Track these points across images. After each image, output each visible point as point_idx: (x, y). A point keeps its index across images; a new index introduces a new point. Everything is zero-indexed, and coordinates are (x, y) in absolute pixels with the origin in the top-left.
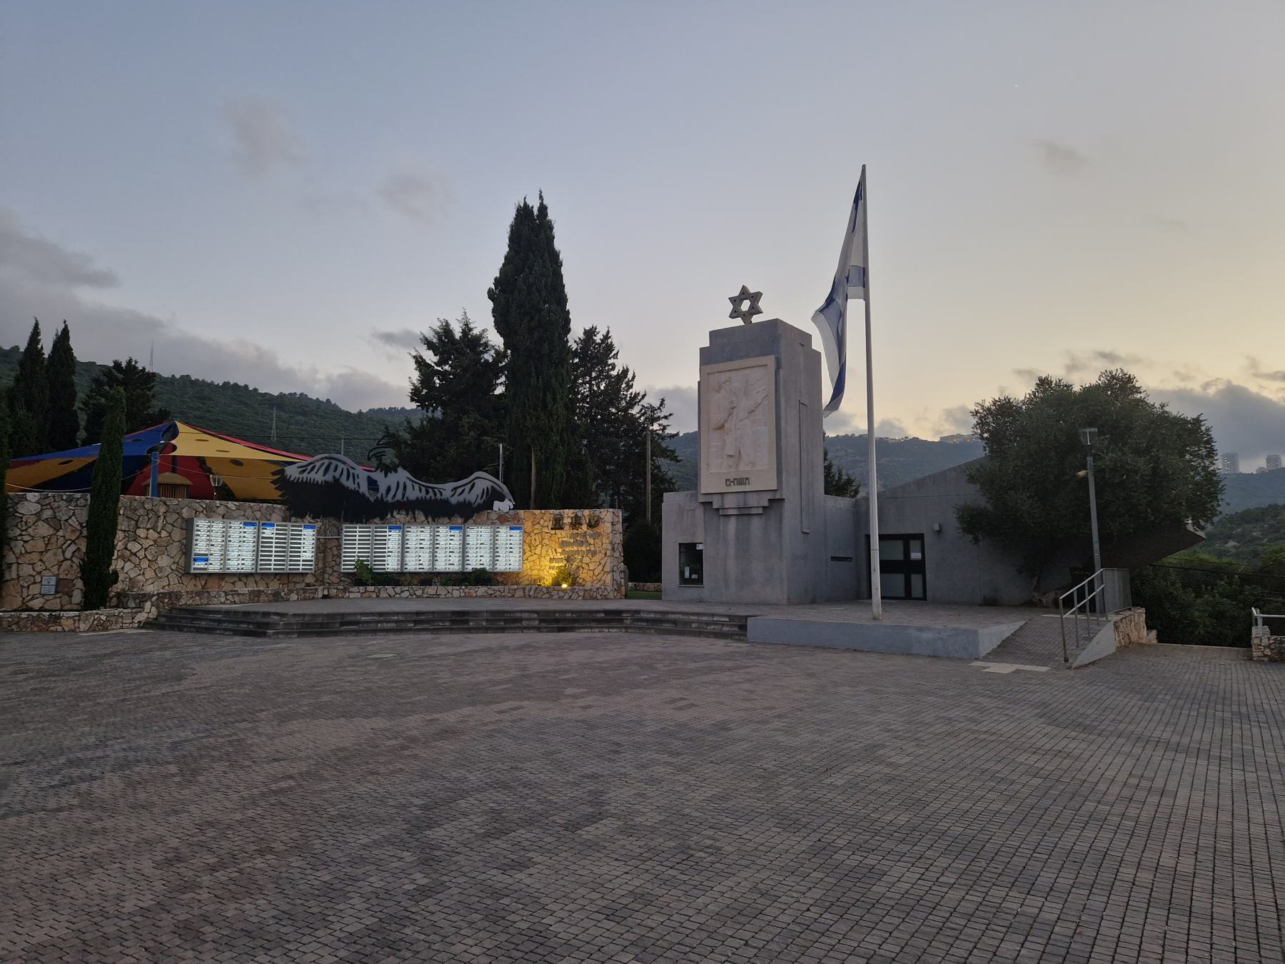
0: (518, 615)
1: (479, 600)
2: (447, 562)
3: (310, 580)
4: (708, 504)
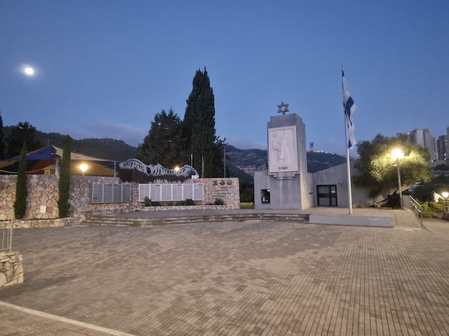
0: (224, 216)
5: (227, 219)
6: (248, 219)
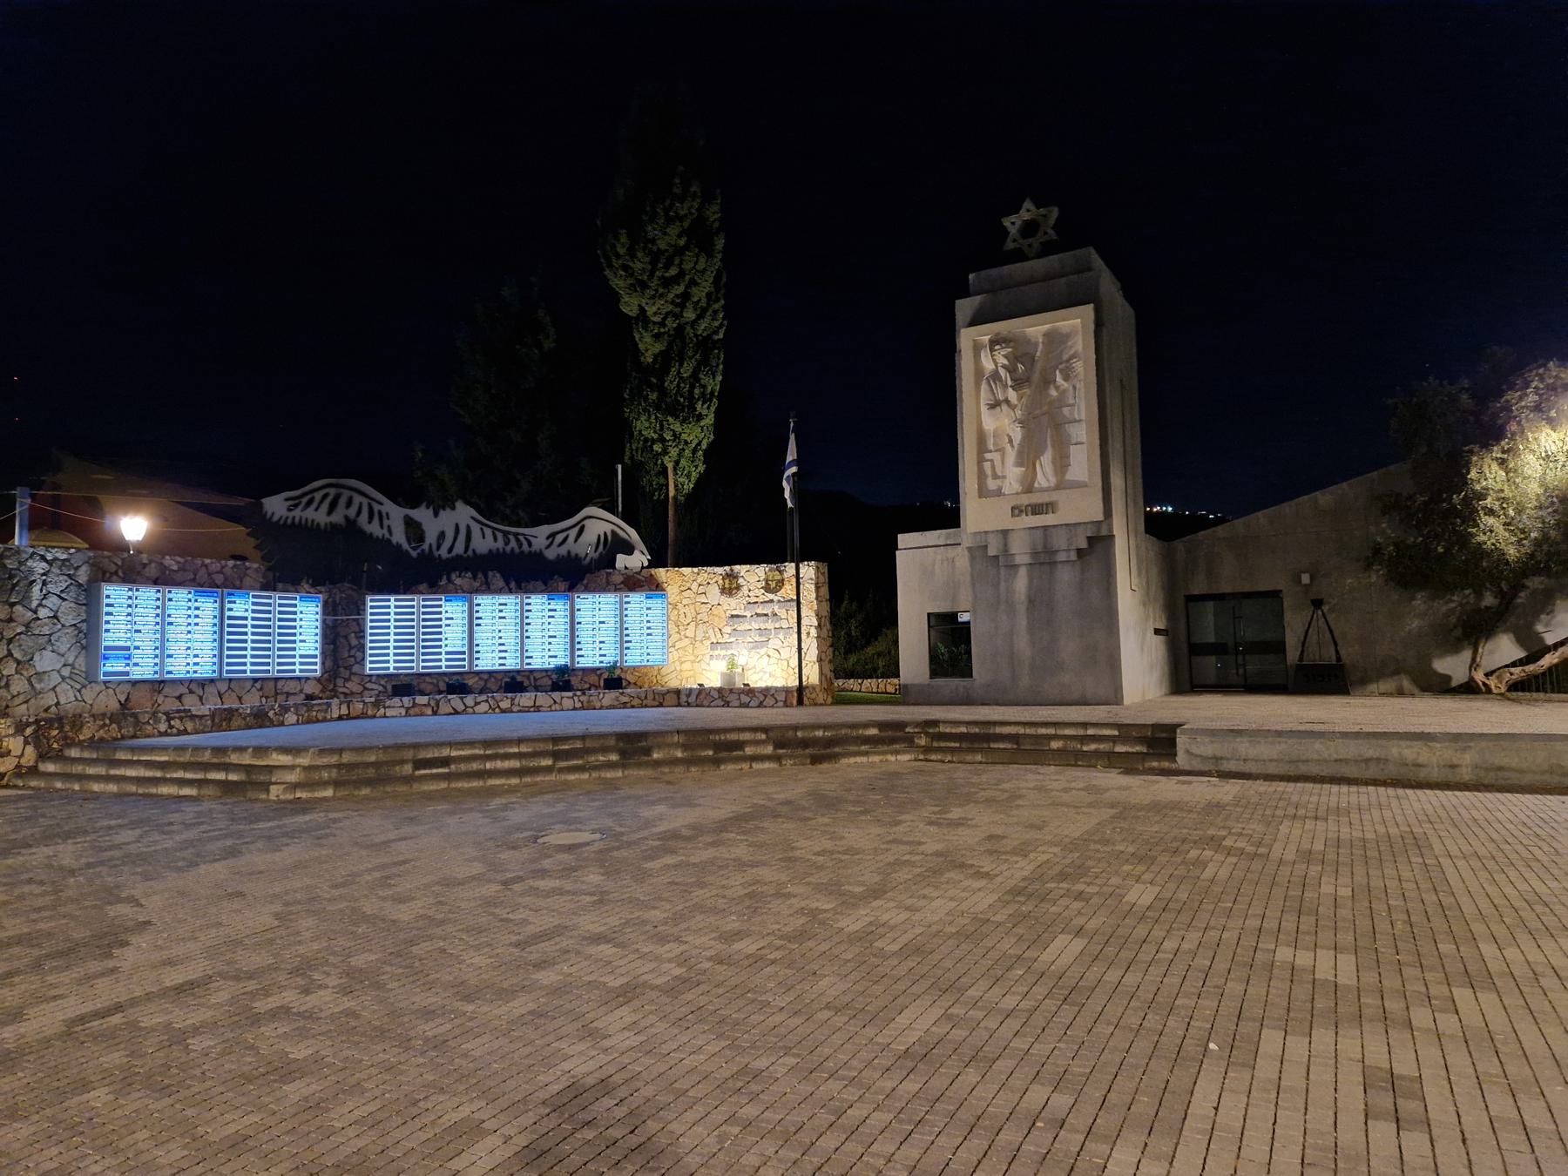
0: (733, 737)
1: (609, 718)
2: (546, 654)
3: (310, 688)
5: (749, 751)
6: (854, 748)
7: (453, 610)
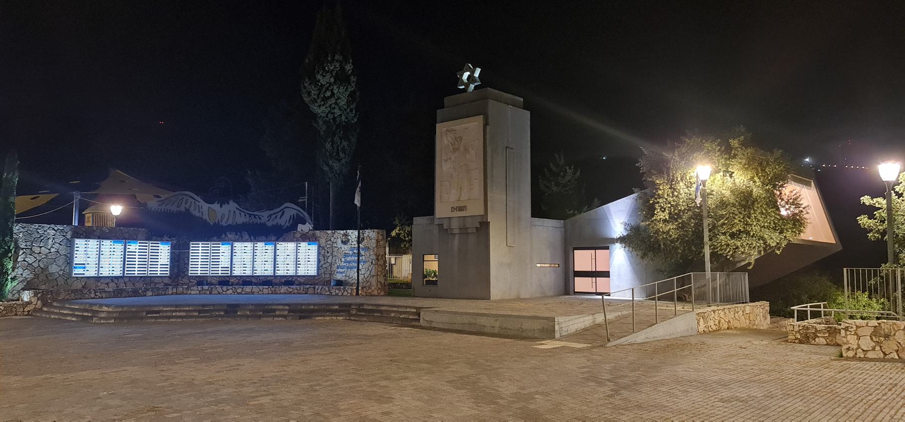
2: (264, 269)
3: (166, 281)
4: (440, 226)
5: (277, 313)
7: (225, 249)
